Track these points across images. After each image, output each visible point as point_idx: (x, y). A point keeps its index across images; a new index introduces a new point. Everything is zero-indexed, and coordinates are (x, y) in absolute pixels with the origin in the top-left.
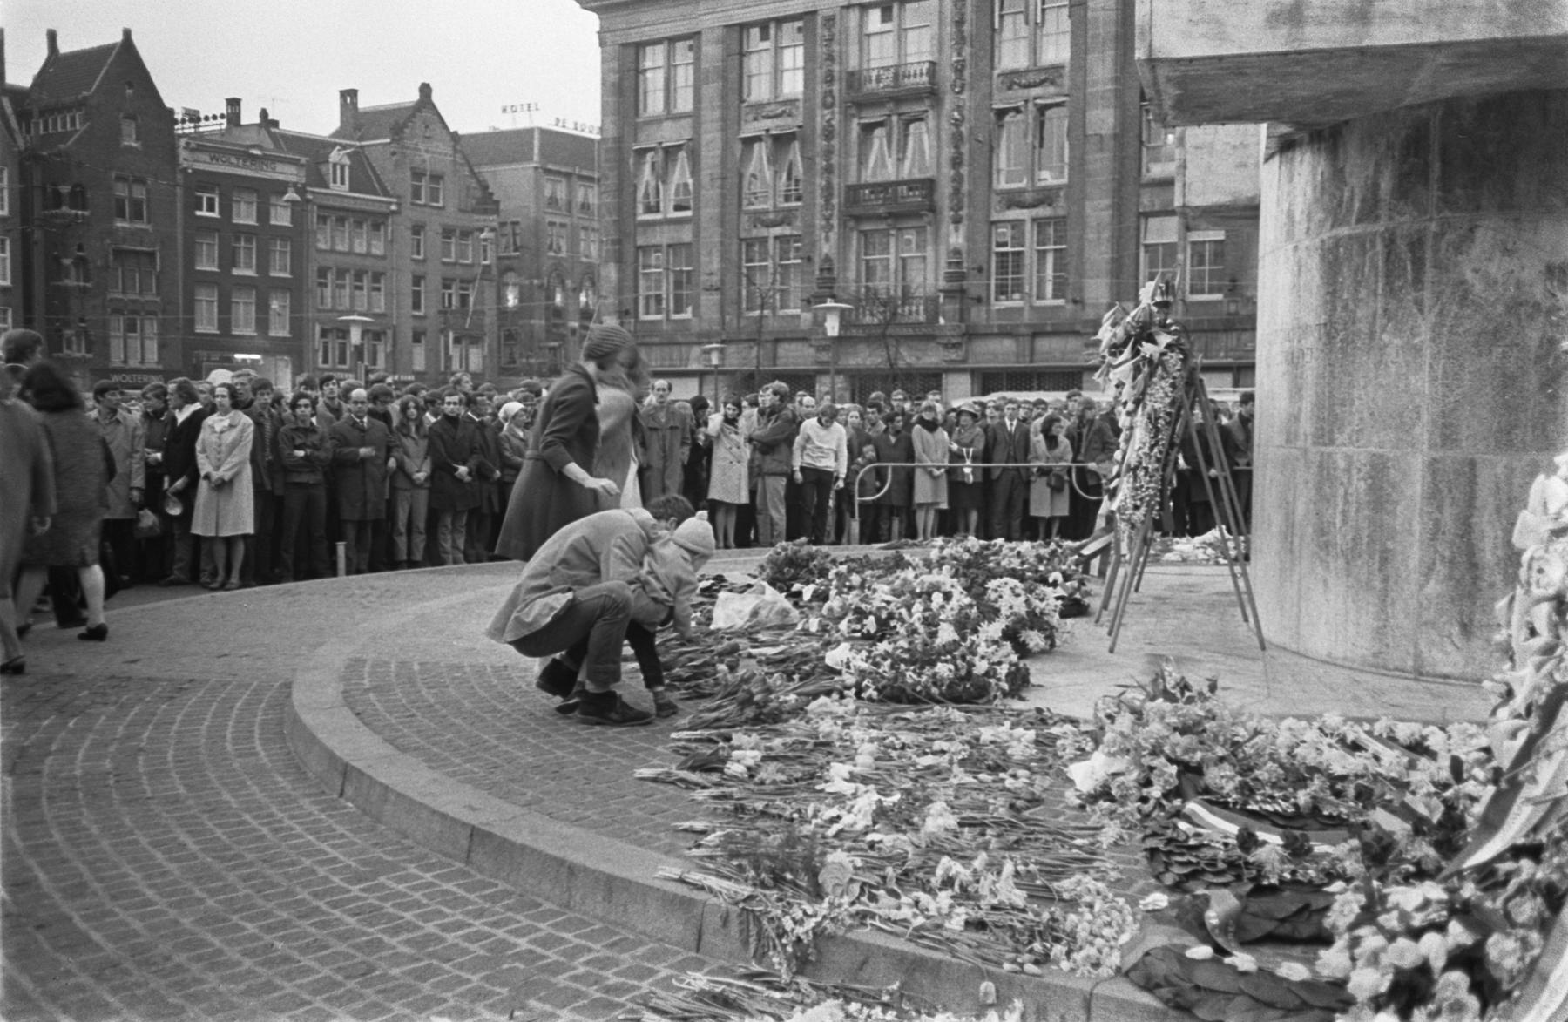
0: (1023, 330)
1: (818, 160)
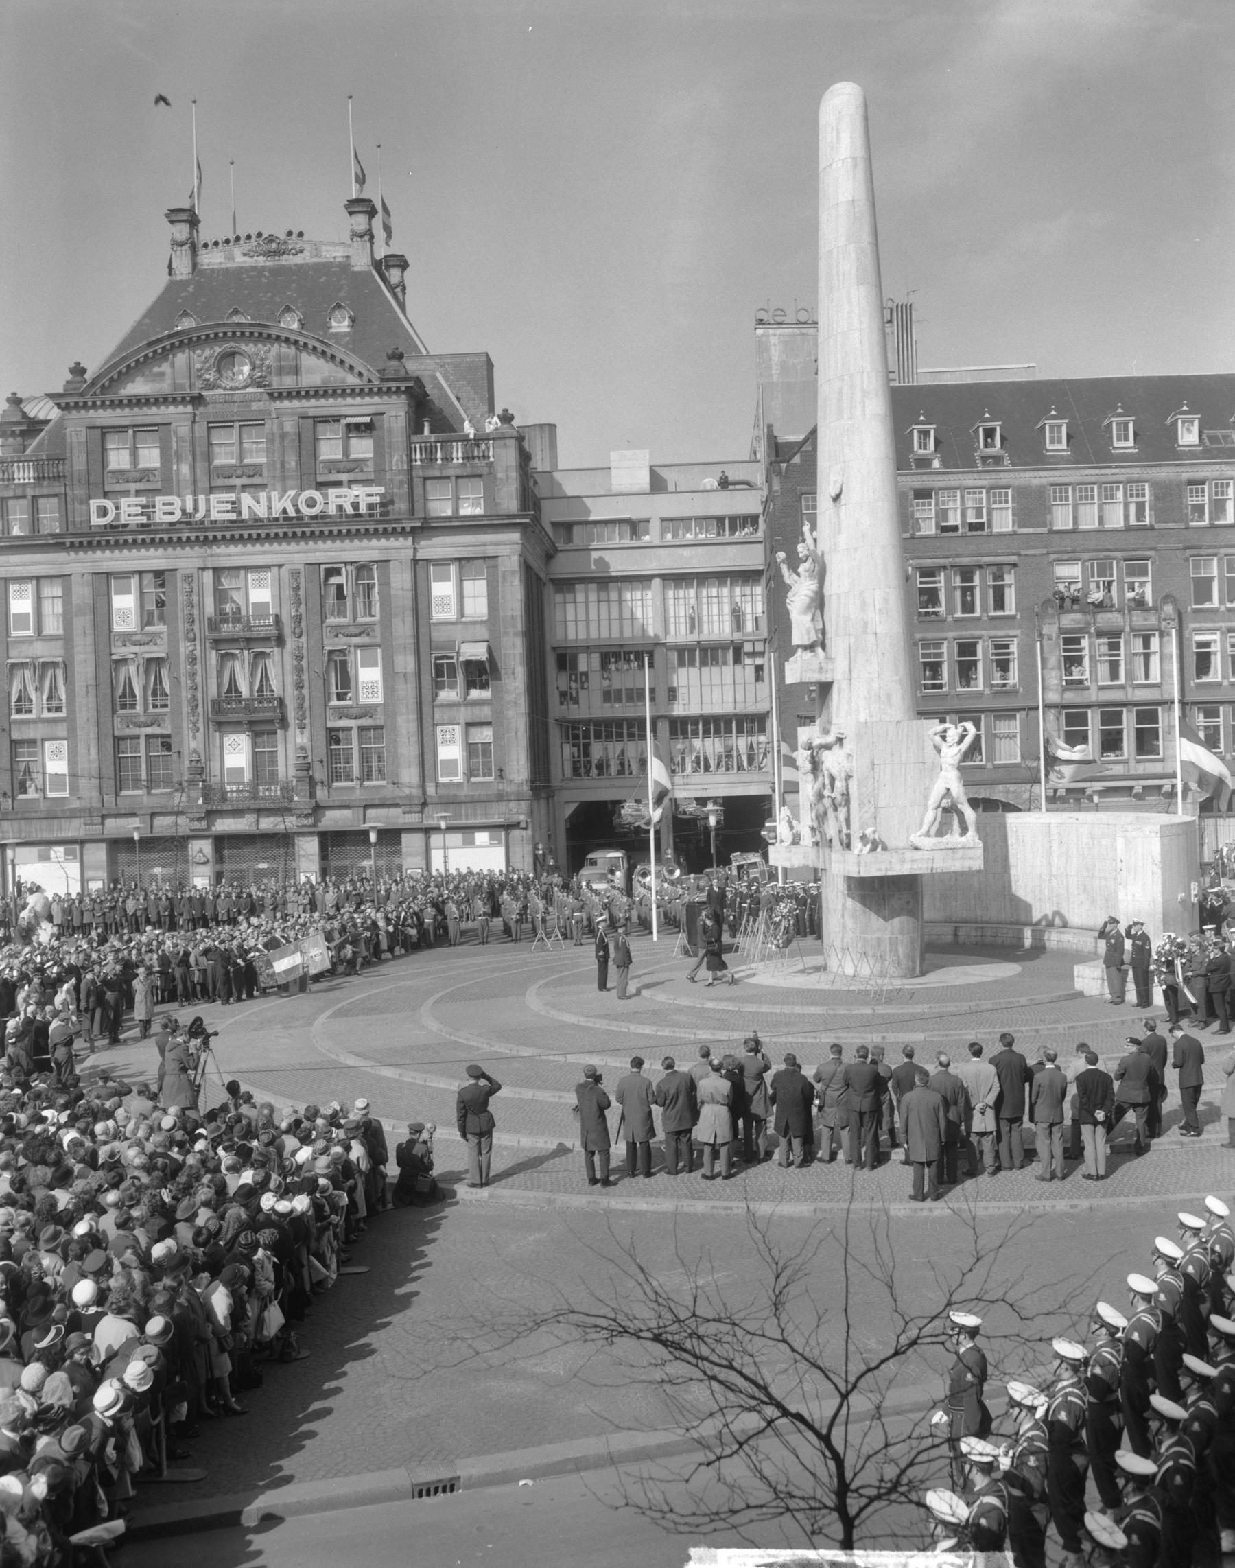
0: (358, 803)
1: (183, 679)
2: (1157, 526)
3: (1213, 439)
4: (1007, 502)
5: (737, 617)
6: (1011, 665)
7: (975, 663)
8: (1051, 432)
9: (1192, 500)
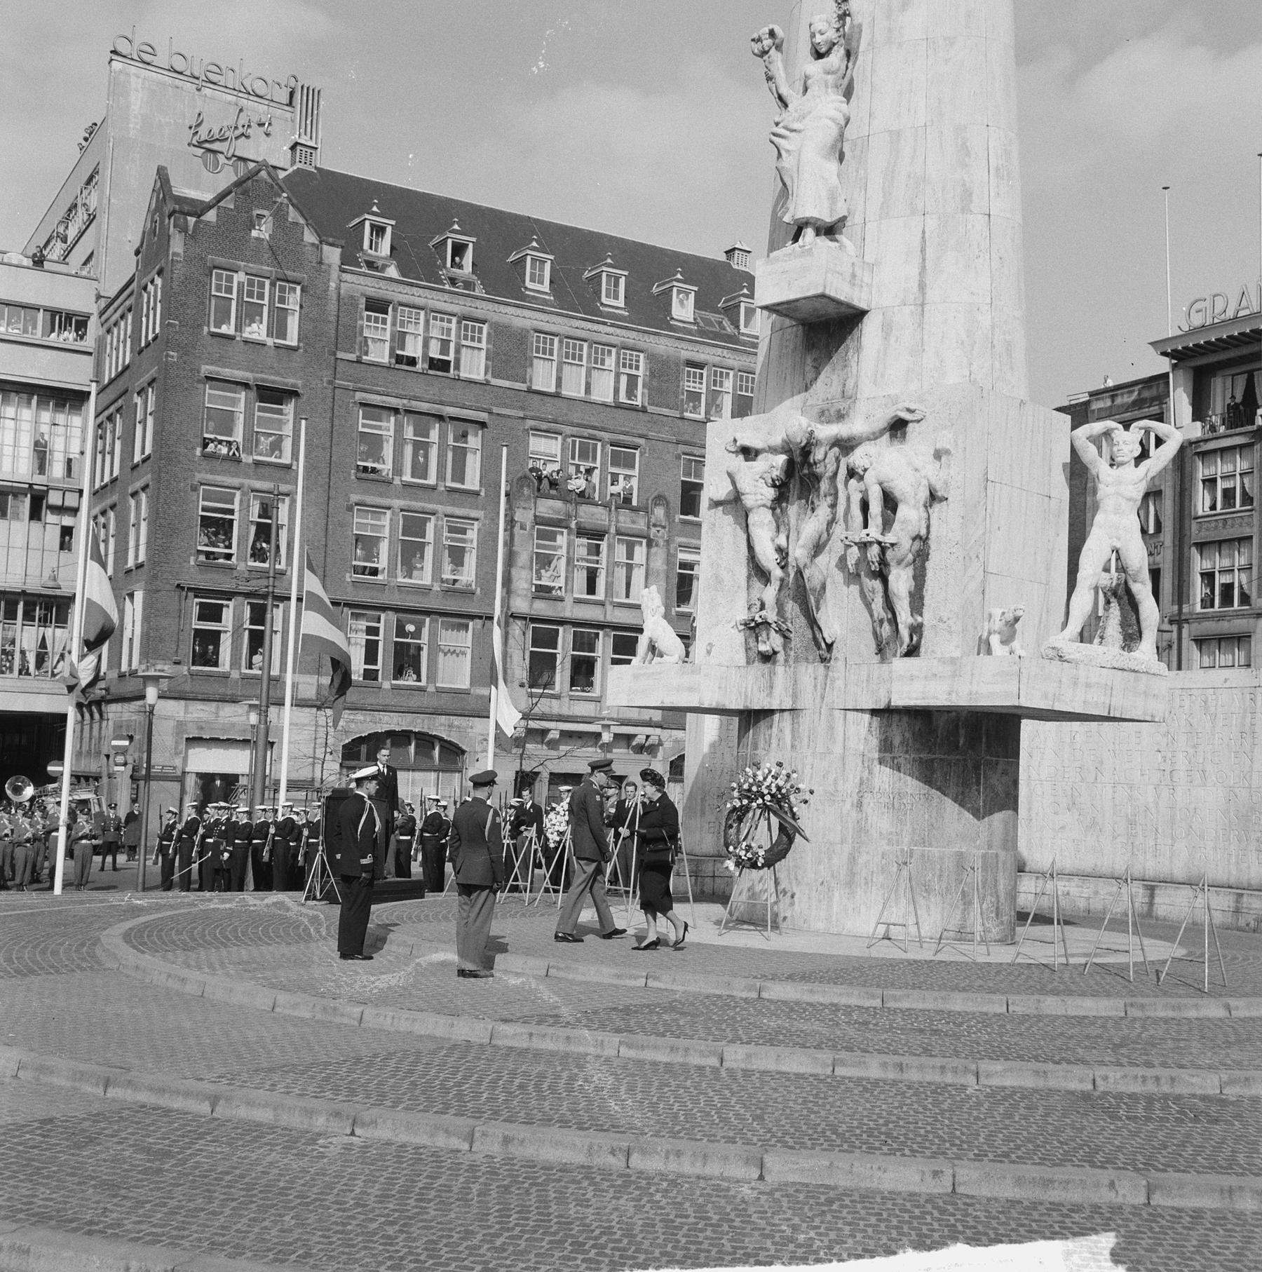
2: (650, 409)
3: (708, 322)
4: (480, 341)
5: (41, 454)
6: (467, 556)
7: (422, 546)
8: (533, 267)
9: (689, 386)
